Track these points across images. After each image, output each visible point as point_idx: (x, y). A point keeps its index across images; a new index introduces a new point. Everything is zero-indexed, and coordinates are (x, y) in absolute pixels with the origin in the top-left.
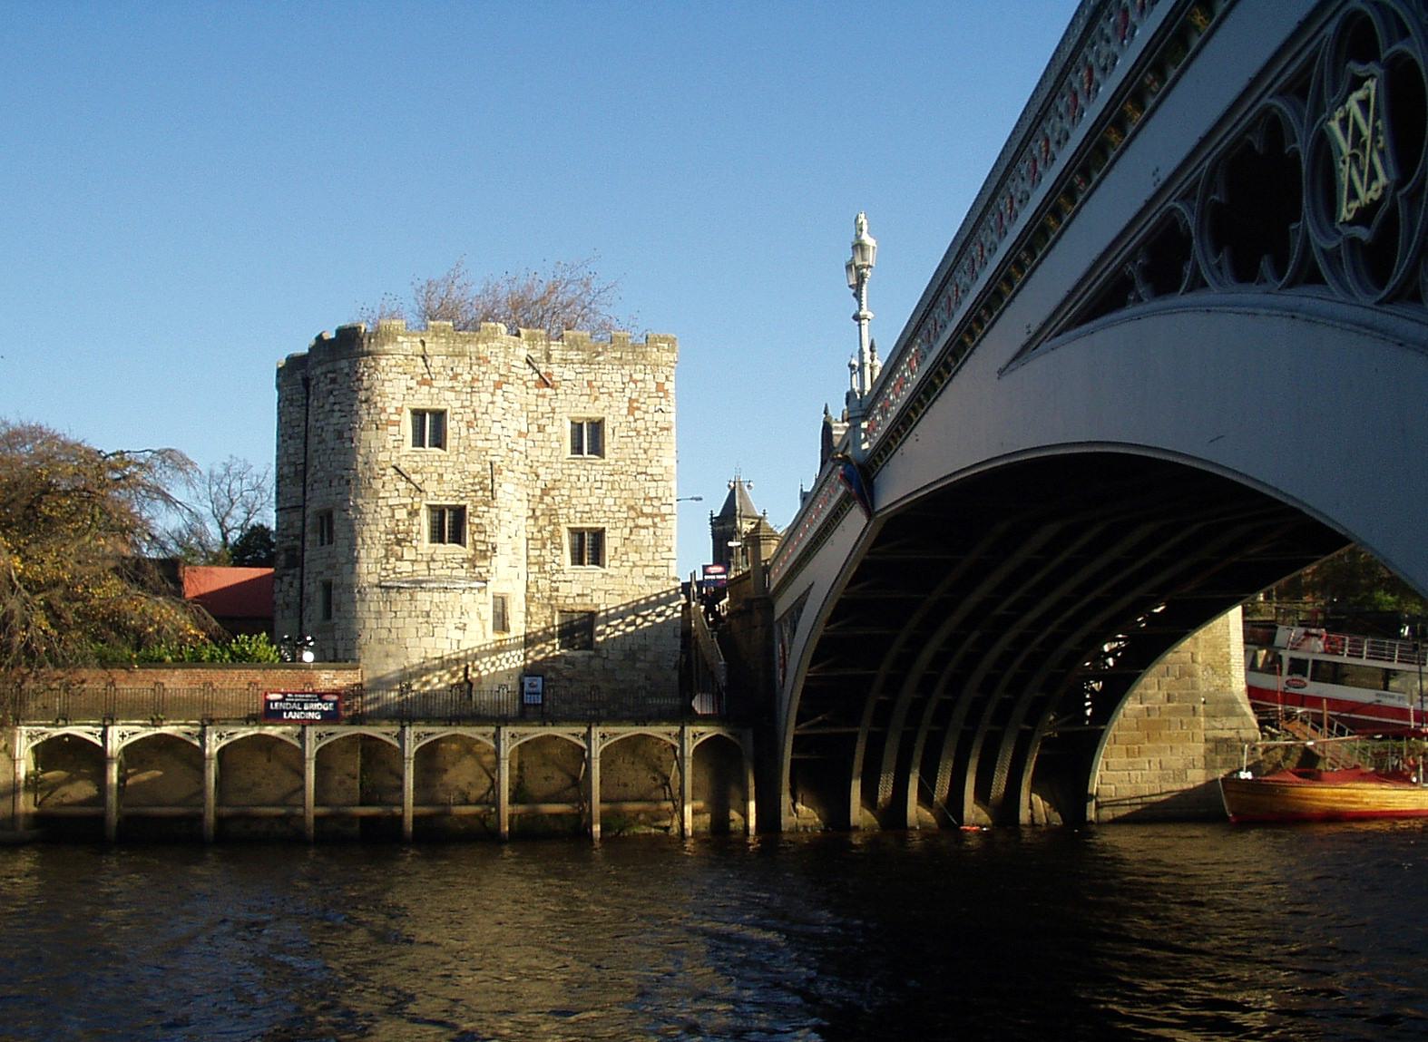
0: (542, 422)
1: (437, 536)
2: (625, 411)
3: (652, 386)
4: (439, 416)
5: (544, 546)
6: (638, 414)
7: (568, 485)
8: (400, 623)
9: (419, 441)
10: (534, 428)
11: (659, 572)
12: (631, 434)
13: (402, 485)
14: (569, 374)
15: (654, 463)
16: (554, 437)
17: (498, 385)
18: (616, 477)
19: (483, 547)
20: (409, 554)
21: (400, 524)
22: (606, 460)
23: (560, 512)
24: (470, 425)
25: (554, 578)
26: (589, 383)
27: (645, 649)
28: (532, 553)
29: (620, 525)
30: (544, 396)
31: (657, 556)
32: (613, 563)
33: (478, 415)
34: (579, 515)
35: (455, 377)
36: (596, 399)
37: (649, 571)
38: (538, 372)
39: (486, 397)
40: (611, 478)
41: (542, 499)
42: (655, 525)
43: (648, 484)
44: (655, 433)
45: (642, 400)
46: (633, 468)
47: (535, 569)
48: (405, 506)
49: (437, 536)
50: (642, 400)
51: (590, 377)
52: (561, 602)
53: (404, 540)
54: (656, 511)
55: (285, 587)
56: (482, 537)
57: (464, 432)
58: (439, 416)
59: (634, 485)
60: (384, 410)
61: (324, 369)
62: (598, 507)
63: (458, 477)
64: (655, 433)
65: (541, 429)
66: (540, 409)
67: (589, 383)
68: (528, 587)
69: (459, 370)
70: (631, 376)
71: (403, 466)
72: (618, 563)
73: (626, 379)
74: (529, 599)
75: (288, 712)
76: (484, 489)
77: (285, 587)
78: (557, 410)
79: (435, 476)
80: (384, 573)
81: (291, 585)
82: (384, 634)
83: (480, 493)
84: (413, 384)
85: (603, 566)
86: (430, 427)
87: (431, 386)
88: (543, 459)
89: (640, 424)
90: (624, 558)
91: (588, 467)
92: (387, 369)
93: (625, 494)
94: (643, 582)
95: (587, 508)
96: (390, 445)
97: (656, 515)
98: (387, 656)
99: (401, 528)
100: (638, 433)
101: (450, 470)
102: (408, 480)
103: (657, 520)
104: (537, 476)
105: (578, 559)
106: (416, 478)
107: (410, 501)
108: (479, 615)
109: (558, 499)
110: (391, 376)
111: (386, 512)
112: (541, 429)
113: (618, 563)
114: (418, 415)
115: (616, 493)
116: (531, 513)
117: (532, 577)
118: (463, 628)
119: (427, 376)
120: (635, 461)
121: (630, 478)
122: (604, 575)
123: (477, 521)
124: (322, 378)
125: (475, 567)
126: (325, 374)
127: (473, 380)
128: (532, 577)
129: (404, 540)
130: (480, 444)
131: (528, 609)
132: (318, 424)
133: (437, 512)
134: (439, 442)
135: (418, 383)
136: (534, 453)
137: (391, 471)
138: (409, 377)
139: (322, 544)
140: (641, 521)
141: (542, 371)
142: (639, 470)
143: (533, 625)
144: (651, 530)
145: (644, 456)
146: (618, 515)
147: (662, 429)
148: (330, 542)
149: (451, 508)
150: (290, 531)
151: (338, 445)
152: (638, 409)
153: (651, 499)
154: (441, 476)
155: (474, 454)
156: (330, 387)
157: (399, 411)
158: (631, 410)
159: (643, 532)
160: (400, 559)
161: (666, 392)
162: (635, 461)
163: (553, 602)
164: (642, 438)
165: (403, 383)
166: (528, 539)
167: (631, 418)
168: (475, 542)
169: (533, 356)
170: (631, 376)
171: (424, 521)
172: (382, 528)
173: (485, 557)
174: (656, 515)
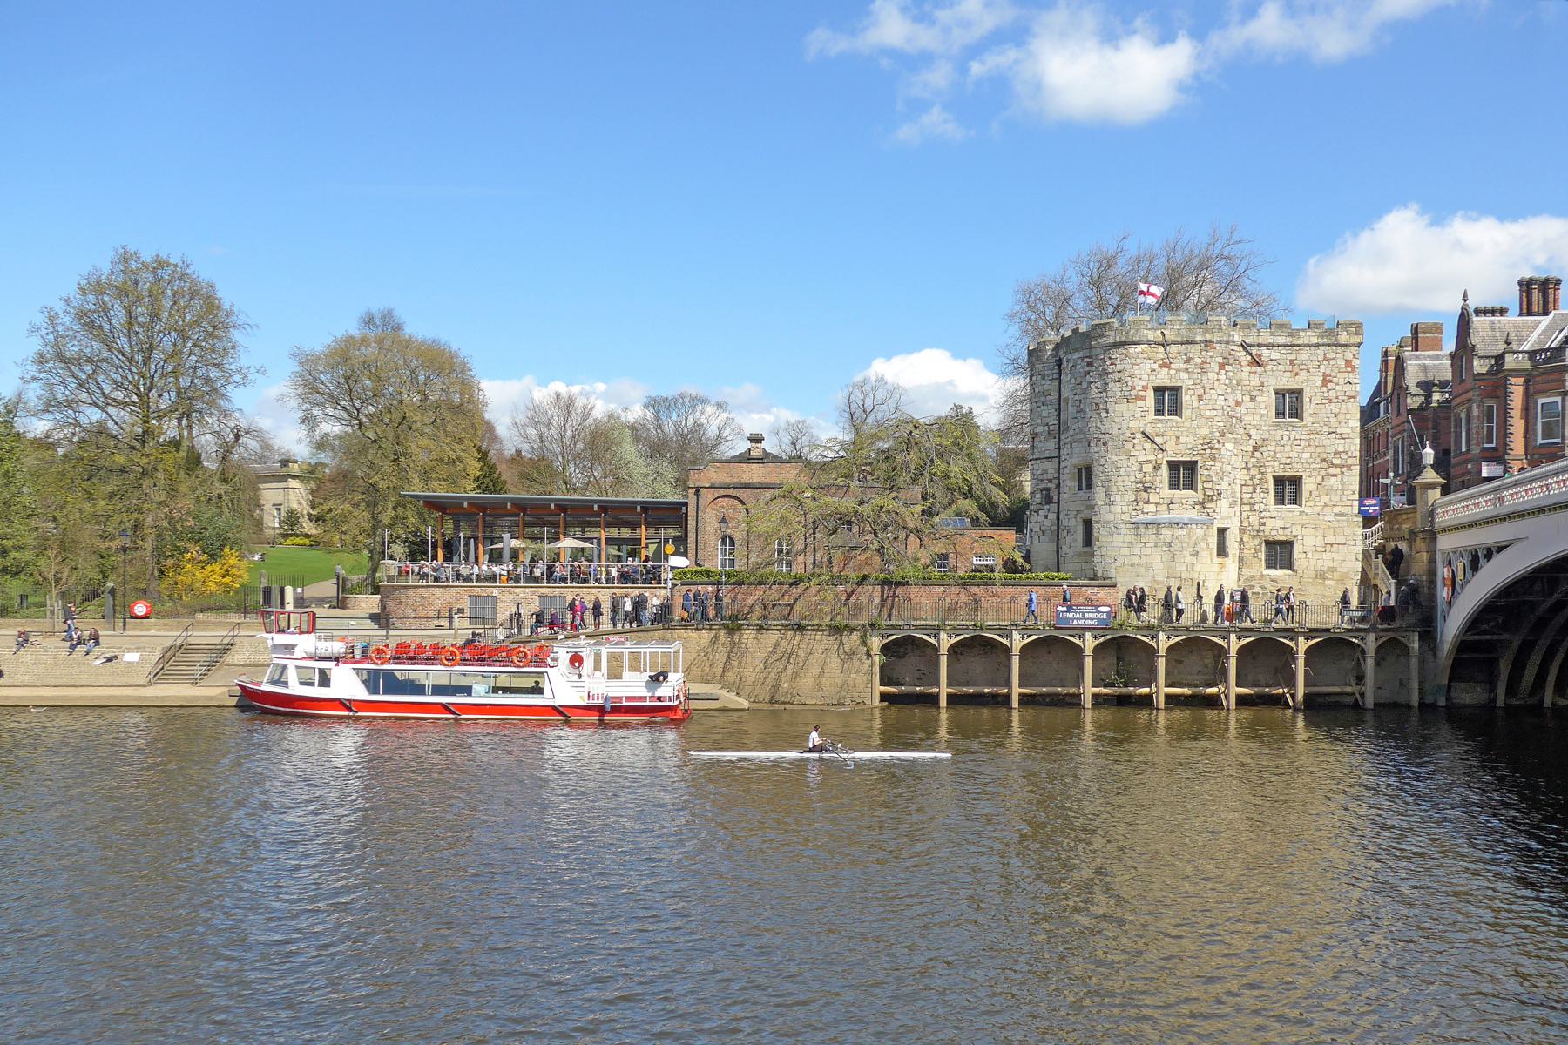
0: (1254, 393)
1: (1174, 484)
2: (1319, 383)
3: (1342, 364)
4: (1176, 391)
5: (1255, 489)
6: (1330, 386)
7: (1273, 443)
8: (1148, 551)
9: (1159, 411)
10: (1247, 398)
11: (1345, 510)
12: (1324, 401)
13: (1148, 446)
14: (1275, 354)
15: (1343, 424)
16: (1263, 406)
17: (1222, 366)
18: (1312, 436)
19: (1211, 493)
20: (1154, 498)
21: (1147, 475)
22: (1305, 423)
23: (1267, 464)
24: (1200, 399)
25: (1262, 515)
26: (1292, 362)
27: (1333, 570)
28: (1245, 496)
29: (1315, 473)
30: (1255, 373)
31: (1344, 498)
32: (1308, 504)
33: (1207, 390)
34: (1282, 466)
35: (1188, 361)
36: (1297, 374)
37: (1337, 510)
38: (1251, 354)
39: (1212, 376)
40: (1308, 437)
41: (1253, 454)
42: (1342, 474)
43: (1337, 441)
44: (1343, 401)
45: (1333, 374)
46: (1326, 429)
47: (1247, 508)
48: (1150, 462)
49: (1174, 484)
50: (1333, 374)
51: (1290, 357)
52: (1267, 533)
53: (1150, 488)
54: (1343, 462)
55: (1041, 518)
56: (1210, 485)
57: (1196, 404)
58: (1176, 391)
59: (1327, 442)
60: (1133, 388)
61: (1081, 355)
62: (1297, 460)
63: (1191, 439)
64: (1343, 401)
65: (1253, 399)
66: (1253, 383)
67: (1292, 362)
68: (1241, 522)
69: (1191, 355)
70: (1325, 355)
71: (1149, 431)
72: (1312, 504)
73: (1321, 358)
74: (1242, 531)
75: (1073, 620)
76: (1211, 448)
77: (1041, 518)
78: (1266, 384)
79: (1174, 439)
80: (1134, 513)
81: (1046, 517)
82: (1135, 559)
83: (1208, 451)
84: (1155, 366)
85: (1301, 506)
86: (1169, 399)
87: (1169, 368)
88: (1255, 422)
89: (1332, 394)
90: (1317, 499)
91: (1290, 428)
92: (1135, 356)
93: (1319, 450)
94: (1332, 518)
95: (1288, 461)
96: (1138, 415)
97: (1344, 466)
98: (1138, 576)
99: (1148, 479)
100: (1330, 401)
101: (1185, 433)
102: (1153, 442)
103: (1344, 469)
104: (1250, 436)
105: (1280, 500)
106: (1159, 440)
107: (1155, 458)
108: (1207, 544)
109: (1265, 454)
110: (1139, 361)
111: (1136, 467)
112: (1253, 399)
113: (1312, 504)
114: (1159, 390)
115: (1311, 449)
116: (1244, 465)
117: (1245, 515)
118: (1196, 555)
119: (1166, 361)
120: (1327, 423)
121: (1323, 437)
122: (1301, 513)
123: (1206, 472)
124: (1079, 362)
125: (1204, 508)
126: (1082, 359)
127: (1203, 363)
128: (1245, 515)
129: (1150, 488)
130: (1208, 413)
131: (1241, 539)
132: (1076, 397)
133: (1174, 466)
134: (1176, 410)
135: (1160, 366)
136: (1247, 418)
137: (1139, 436)
138: (1152, 361)
139: (1080, 489)
140: (1332, 471)
141: (1254, 352)
142: (1331, 430)
143: (1245, 551)
144: (1339, 477)
145: (1335, 419)
146: (1313, 466)
147: (1350, 397)
148: (1089, 487)
149: (1185, 463)
150: (1045, 477)
151: (1095, 417)
152: (1331, 381)
153: (1340, 453)
154: (1178, 438)
155: (1203, 421)
156: (1087, 369)
157: (1145, 389)
158: (1326, 382)
159: (1333, 479)
160: (1147, 502)
161: (1353, 368)
162: (1327, 423)
163: (1261, 534)
164: (1333, 405)
165: (1148, 366)
166: (1242, 485)
167: (1325, 389)
168: (1204, 488)
169: (1247, 341)
170: (1325, 355)
171: (1165, 471)
172: (1133, 479)
173: (1212, 501)
174: (1344, 466)
